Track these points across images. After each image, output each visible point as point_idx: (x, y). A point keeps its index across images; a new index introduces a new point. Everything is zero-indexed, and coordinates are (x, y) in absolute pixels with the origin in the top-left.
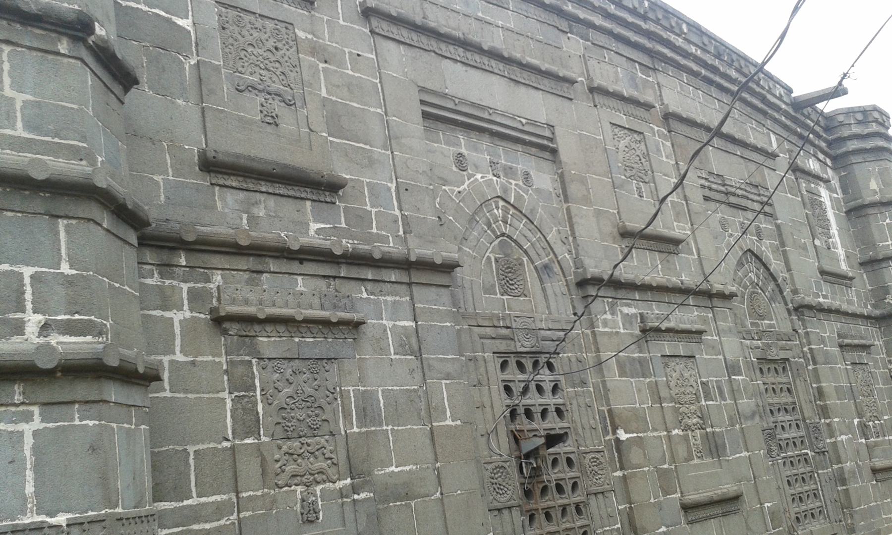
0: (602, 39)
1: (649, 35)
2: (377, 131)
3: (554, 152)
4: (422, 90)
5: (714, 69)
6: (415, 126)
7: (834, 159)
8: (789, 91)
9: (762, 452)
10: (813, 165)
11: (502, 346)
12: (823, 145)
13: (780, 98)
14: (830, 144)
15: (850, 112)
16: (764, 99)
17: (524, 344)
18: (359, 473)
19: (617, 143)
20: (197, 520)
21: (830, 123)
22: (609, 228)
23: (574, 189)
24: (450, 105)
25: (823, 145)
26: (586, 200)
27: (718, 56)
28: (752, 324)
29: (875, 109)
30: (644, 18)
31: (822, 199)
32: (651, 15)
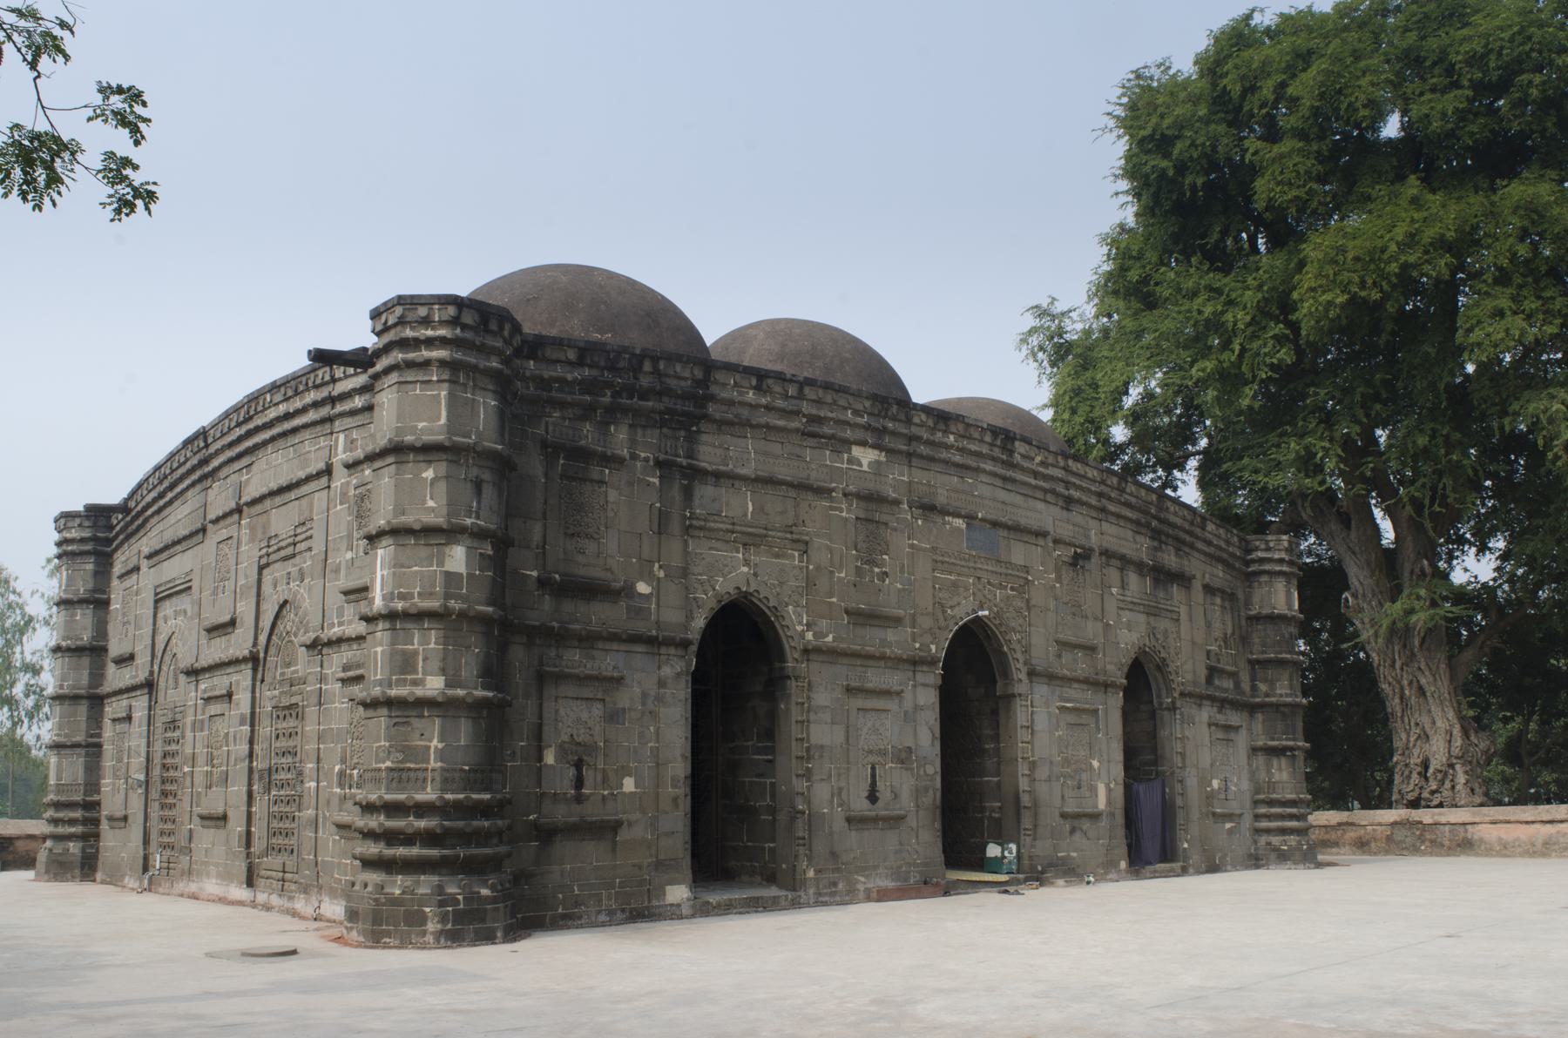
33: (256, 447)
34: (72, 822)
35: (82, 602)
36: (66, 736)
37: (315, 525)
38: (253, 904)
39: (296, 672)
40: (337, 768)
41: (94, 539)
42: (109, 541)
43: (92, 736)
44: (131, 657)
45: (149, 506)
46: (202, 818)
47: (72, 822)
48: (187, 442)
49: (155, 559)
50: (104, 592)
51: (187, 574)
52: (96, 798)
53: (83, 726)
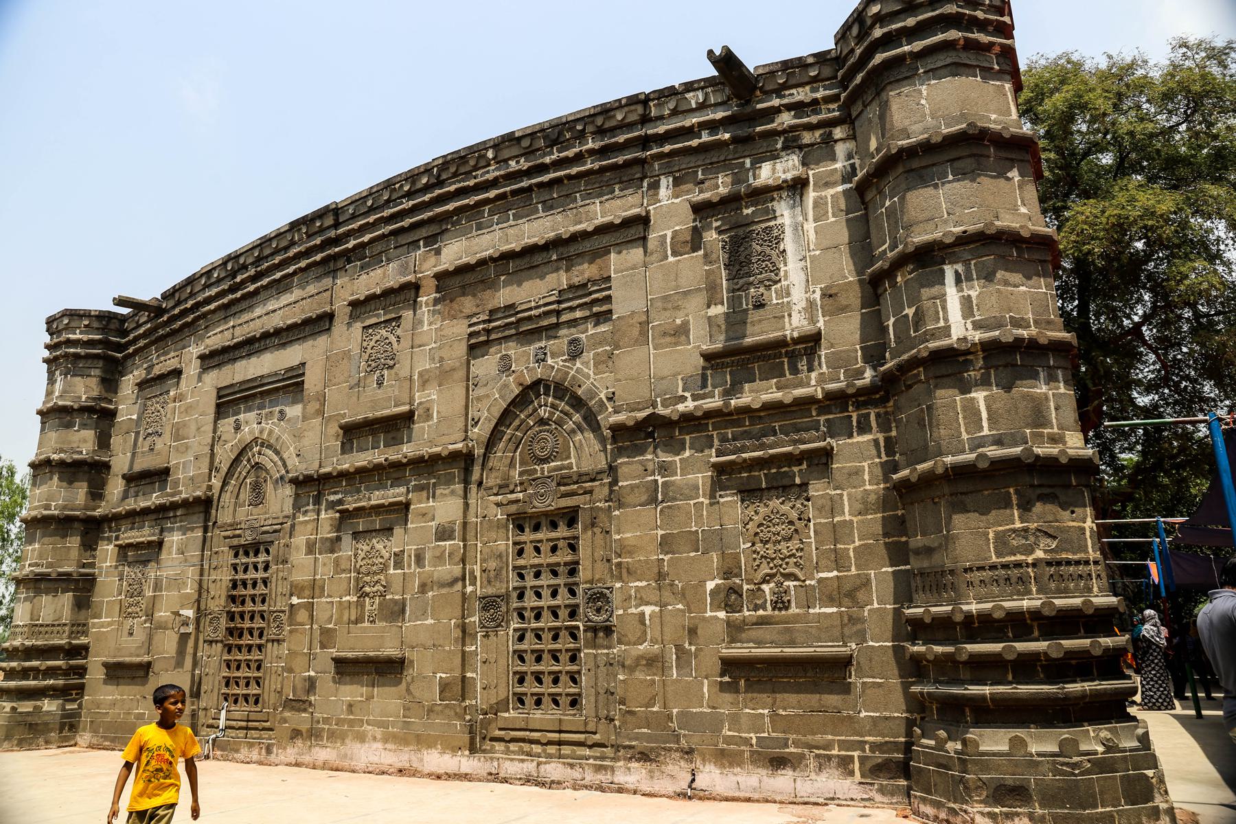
0: (379, 247)
2: (193, 427)
4: (219, 390)
9: (453, 622)
11: (235, 542)
13: (702, 106)
17: (248, 538)
18: (150, 616)
19: (365, 344)
20: (103, 627)
22: (334, 429)
24: (236, 389)
28: (521, 474)
30: (440, 183)
31: (779, 221)
32: (444, 176)
33: (446, 217)
34: (51, 672)
35: (83, 410)
36: (50, 565)
37: (613, 283)
38: (494, 777)
39: (570, 467)
40: (710, 585)
41: (105, 343)
42: (120, 348)
43: (84, 566)
44: (166, 472)
45: (208, 301)
46: (339, 662)
47: (51, 672)
48: (294, 225)
49: (216, 360)
50: (110, 402)
51: (292, 369)
52: (83, 640)
53: (74, 554)
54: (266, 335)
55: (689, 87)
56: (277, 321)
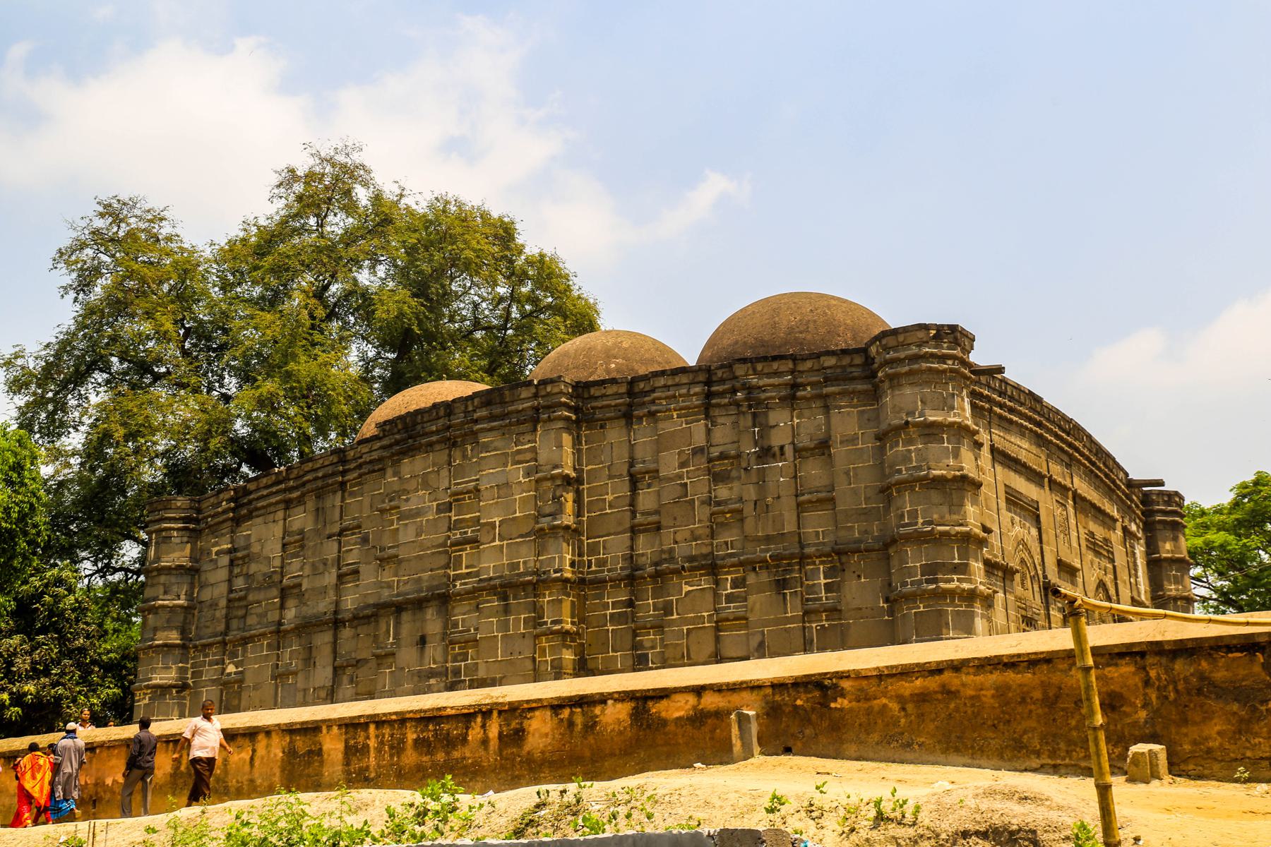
1: (1070, 445)
3: (1038, 516)
5: (1093, 464)
6: (1003, 504)
7: (1145, 524)
8: (1127, 474)
10: (1134, 528)
12: (1139, 512)
14: (1143, 513)
15: (1161, 493)
16: (1114, 482)
21: (1146, 499)
23: (1044, 536)
25: (1139, 512)
26: (1048, 544)
27: (1096, 455)
29: (1177, 493)
54: (1024, 465)
55: (1122, 470)
56: (1023, 456)
